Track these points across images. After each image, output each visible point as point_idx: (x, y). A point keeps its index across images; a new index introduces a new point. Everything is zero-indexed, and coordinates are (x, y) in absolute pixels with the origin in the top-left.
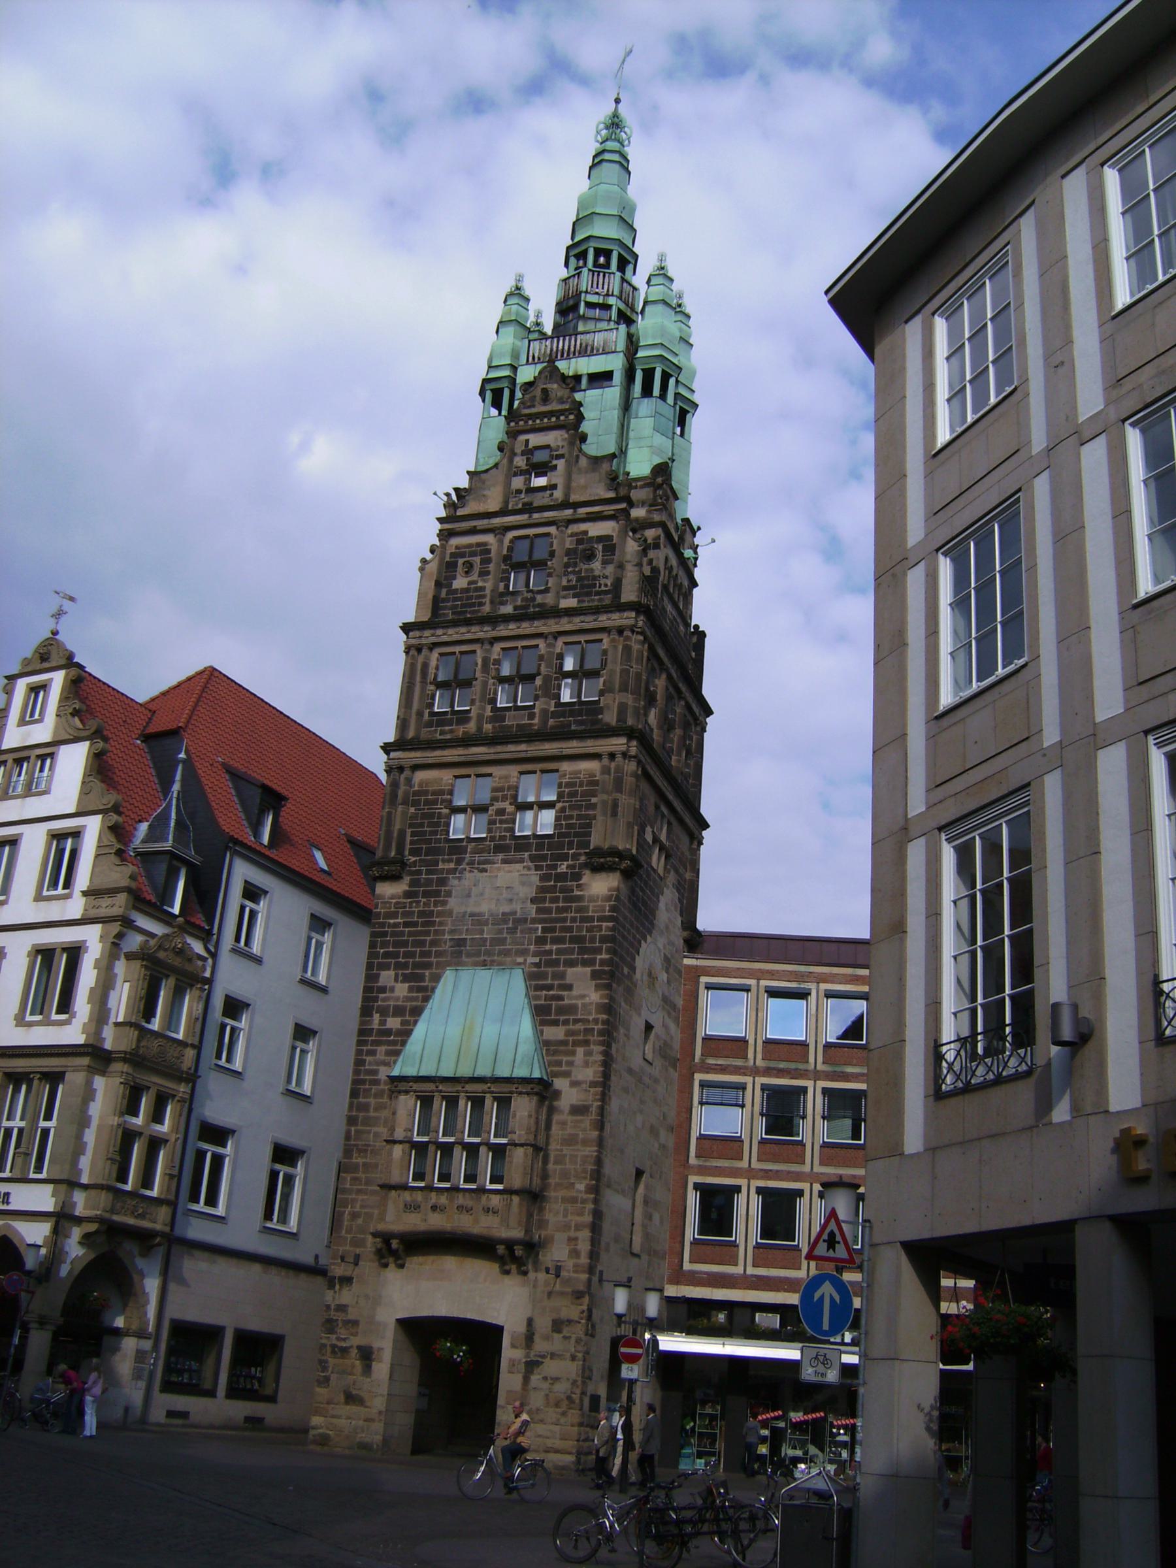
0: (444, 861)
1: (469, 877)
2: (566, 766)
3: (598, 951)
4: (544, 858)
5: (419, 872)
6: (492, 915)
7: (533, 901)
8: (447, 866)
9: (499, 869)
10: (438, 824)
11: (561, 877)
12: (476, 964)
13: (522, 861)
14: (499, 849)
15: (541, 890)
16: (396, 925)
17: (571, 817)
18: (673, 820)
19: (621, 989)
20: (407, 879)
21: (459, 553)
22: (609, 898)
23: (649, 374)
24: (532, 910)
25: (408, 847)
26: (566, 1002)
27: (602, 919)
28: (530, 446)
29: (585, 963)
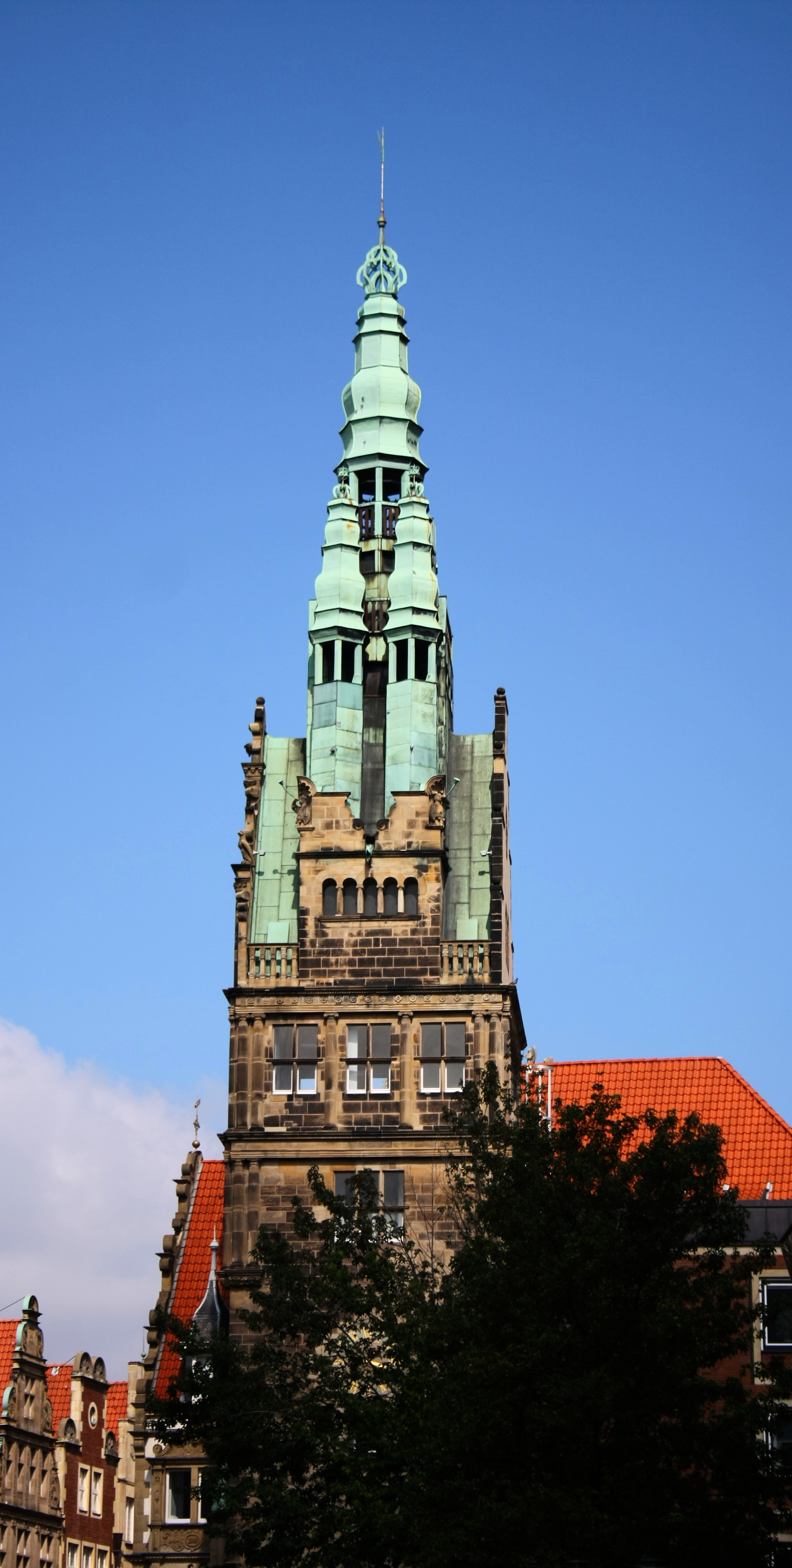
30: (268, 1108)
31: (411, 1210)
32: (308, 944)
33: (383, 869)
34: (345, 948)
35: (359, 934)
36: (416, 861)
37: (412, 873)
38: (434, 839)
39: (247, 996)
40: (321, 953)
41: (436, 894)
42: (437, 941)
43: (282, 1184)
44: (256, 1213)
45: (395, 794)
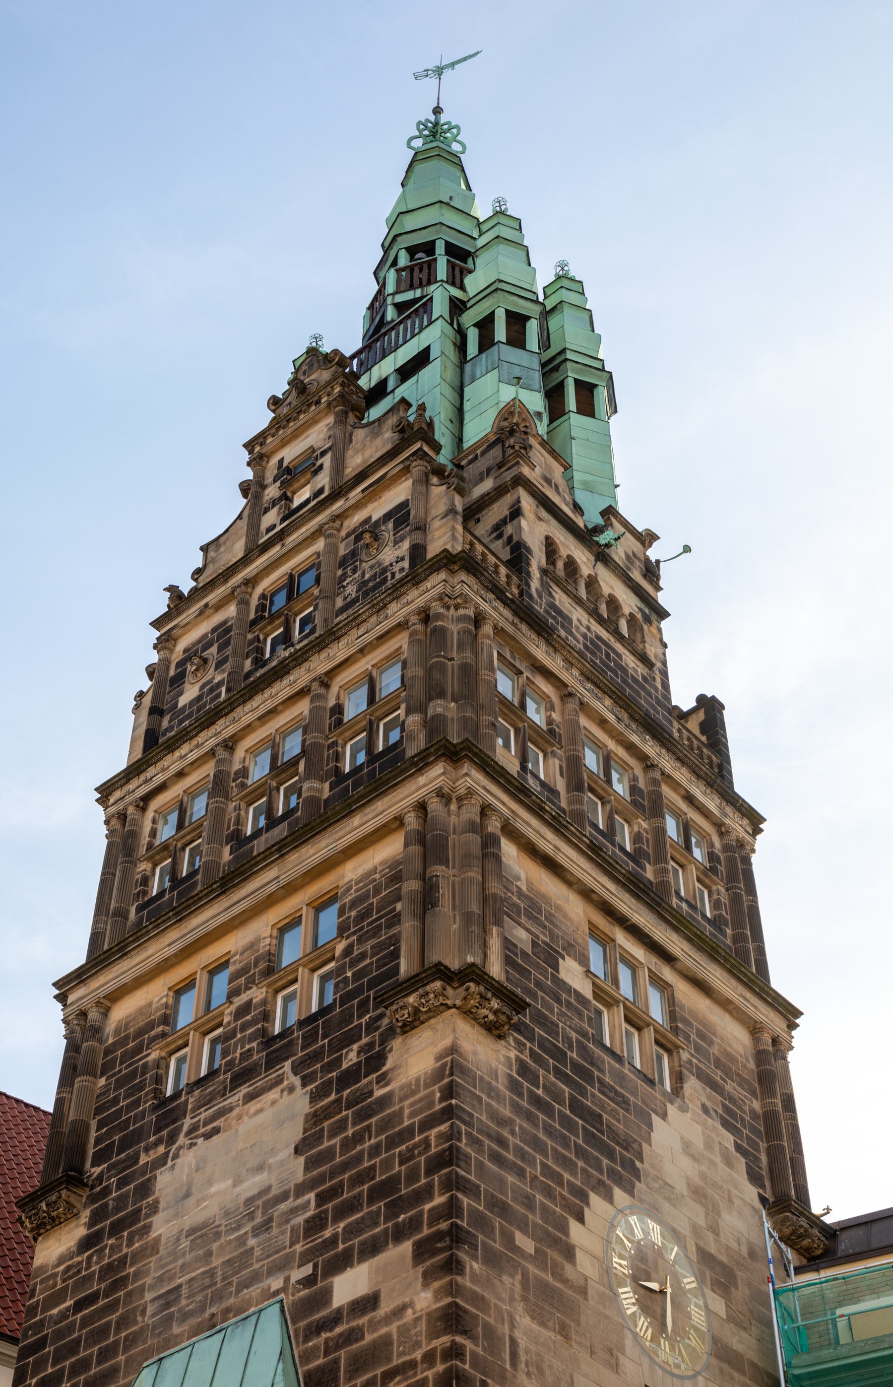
0: (147, 1150)
1: (188, 1159)
2: (352, 871)
3: (426, 1193)
4: (316, 1056)
5: (106, 1191)
6: (227, 1214)
7: (297, 1151)
8: (153, 1155)
9: (239, 1117)
10: (140, 1087)
11: (351, 1076)
12: (196, 1331)
13: (279, 1081)
14: (239, 1079)
15: (315, 1119)
16: (63, 1315)
17: (363, 956)
18: (667, 974)
19: (510, 1283)
20: (85, 1215)
21: (190, 654)
22: (438, 1074)
23: (486, 325)
24: (297, 1170)
25: (91, 1151)
26: (369, 1338)
27: (426, 1125)
28: (285, 464)
29: (399, 1235)
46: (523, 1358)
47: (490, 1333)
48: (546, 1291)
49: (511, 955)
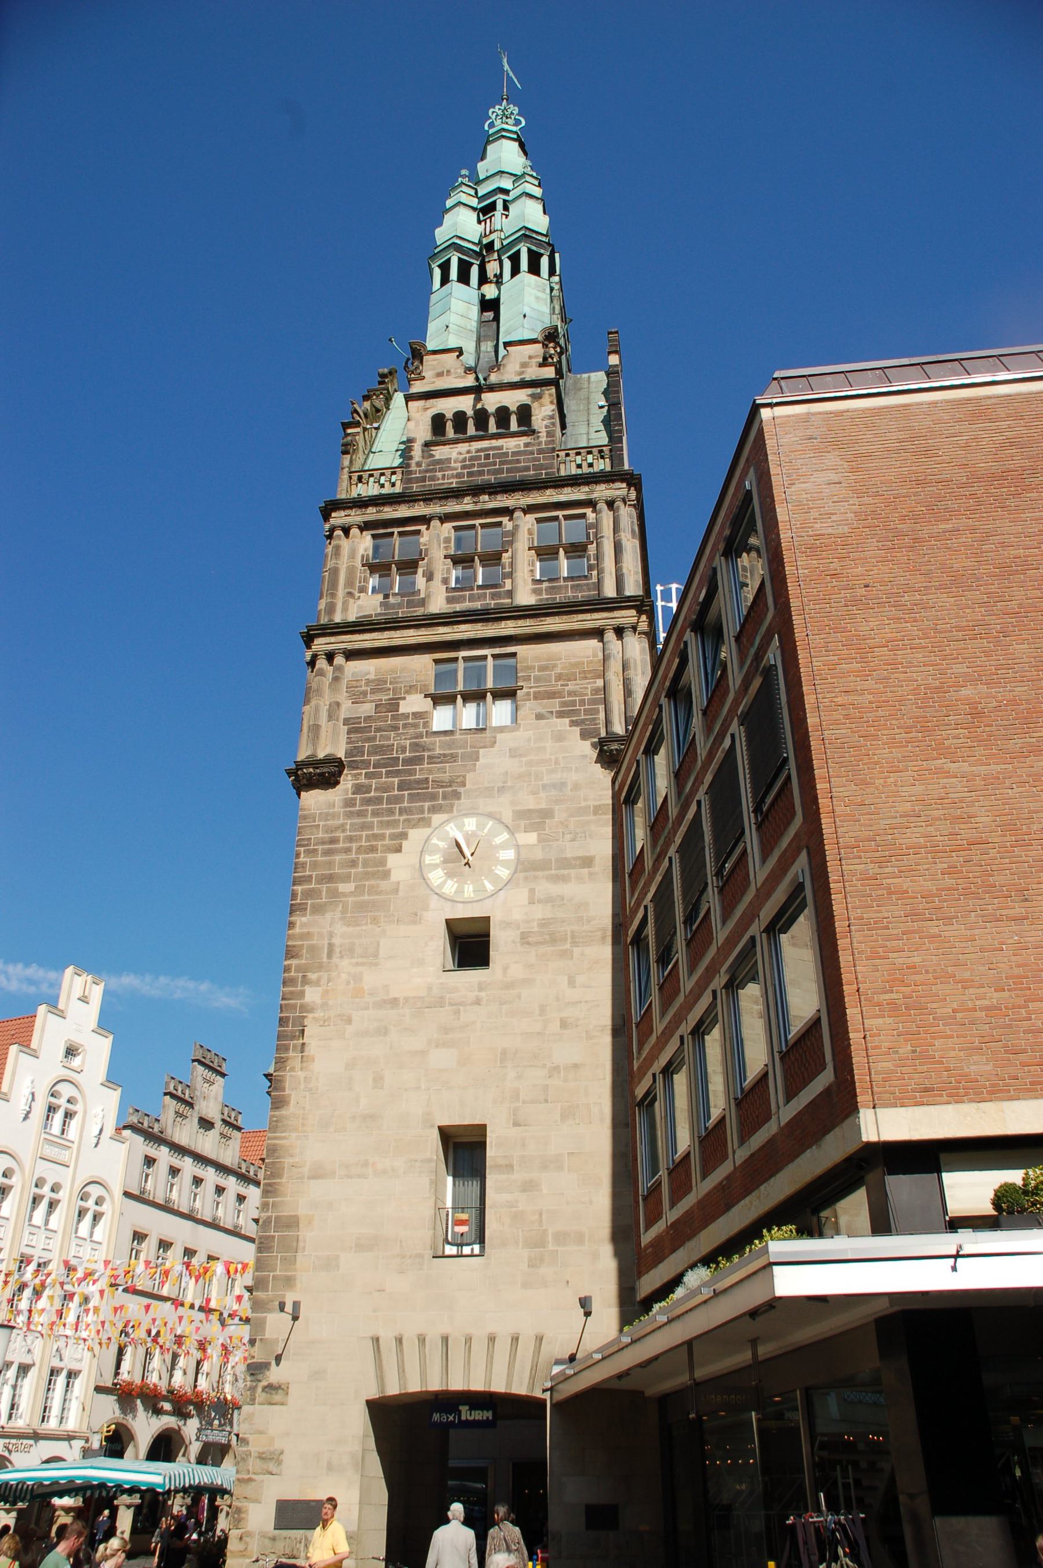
30: (360, 607)
31: (524, 690)
32: (413, 465)
33: (492, 401)
34: (453, 465)
35: (468, 452)
36: (530, 391)
37: (527, 401)
38: (549, 373)
39: (344, 509)
40: (426, 471)
41: (551, 413)
42: (553, 450)
43: (372, 677)
44: (338, 704)
45: (507, 344)
46: (337, 950)
47: (313, 949)
48: (362, 906)
49: (354, 727)
